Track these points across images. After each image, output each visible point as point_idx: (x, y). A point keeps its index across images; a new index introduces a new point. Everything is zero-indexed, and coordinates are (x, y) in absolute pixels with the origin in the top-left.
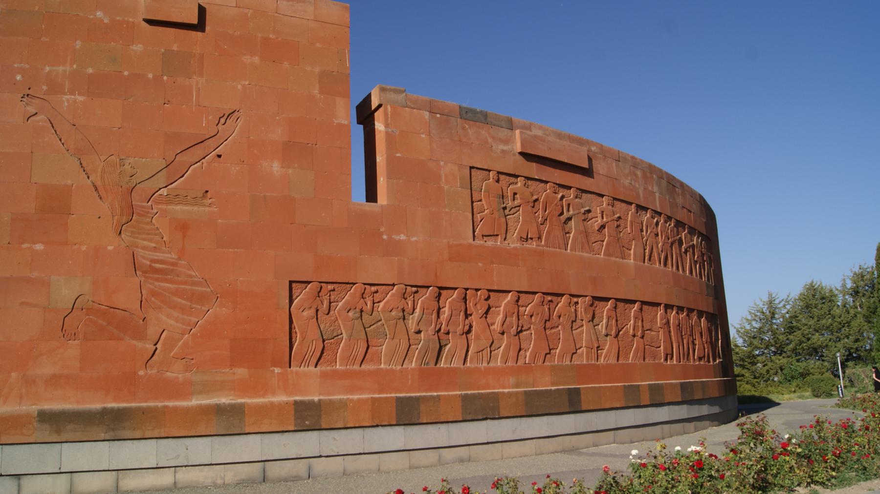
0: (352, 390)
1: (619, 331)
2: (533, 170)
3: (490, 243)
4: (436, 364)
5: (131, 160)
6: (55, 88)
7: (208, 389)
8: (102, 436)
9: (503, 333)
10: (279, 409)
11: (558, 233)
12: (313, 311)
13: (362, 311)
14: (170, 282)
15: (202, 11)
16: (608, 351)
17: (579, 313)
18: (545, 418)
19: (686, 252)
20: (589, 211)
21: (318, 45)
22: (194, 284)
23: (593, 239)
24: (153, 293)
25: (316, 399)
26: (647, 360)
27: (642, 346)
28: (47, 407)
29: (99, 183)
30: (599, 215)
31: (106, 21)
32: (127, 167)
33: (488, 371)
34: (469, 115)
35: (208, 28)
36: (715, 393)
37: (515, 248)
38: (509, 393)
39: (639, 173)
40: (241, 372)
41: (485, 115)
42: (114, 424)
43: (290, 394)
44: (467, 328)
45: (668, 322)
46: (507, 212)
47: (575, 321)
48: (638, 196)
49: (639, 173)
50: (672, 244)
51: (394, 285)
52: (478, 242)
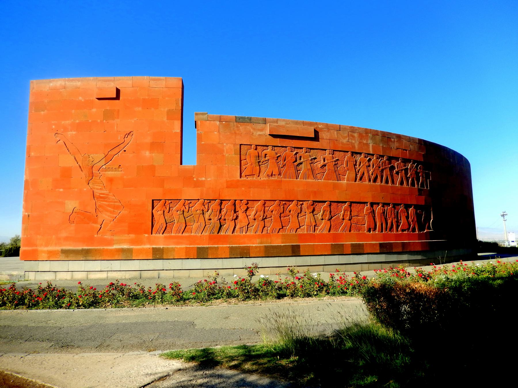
0: (178, 244)
1: (331, 218)
2: (278, 142)
3: (250, 178)
4: (218, 233)
5: (92, 155)
6: (66, 129)
7: (119, 242)
8: (82, 259)
9: (255, 219)
10: (146, 251)
11: (292, 171)
12: (162, 212)
13: (183, 211)
14: (106, 201)
15: (118, 91)
16: (322, 227)
17: (303, 210)
19: (397, 173)
20: (315, 158)
21: (167, 98)
22: (115, 202)
23: (317, 172)
24: (100, 206)
25: (162, 247)
26: (352, 232)
27: (349, 224)
28: (65, 248)
29: (81, 165)
30: (322, 160)
31: (83, 100)
32: (91, 158)
33: (244, 237)
34: (241, 120)
35: (121, 98)
36: (419, 249)
37: (264, 180)
39: (356, 135)
40: (132, 236)
41: (250, 119)
42: (86, 255)
43: (151, 244)
44: (235, 217)
45: (373, 212)
46: (260, 163)
47: (301, 213)
48: (354, 147)
49: (356, 135)
50: (382, 171)
51: (199, 200)
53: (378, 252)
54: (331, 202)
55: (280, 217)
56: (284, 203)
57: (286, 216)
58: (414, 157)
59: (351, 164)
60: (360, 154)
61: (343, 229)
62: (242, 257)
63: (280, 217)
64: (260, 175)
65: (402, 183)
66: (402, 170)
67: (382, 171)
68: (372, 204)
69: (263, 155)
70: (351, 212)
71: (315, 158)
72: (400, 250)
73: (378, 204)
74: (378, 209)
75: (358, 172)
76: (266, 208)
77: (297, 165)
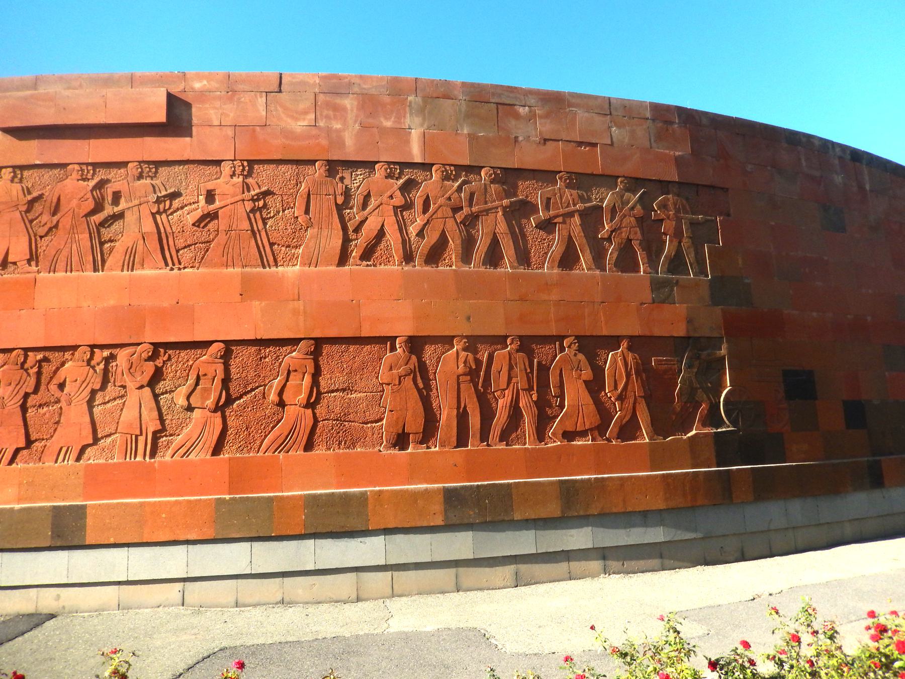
1: (230, 401)
19: (547, 226)
23: (180, 243)
26: (319, 451)
39: (349, 103)
47: (103, 387)
48: (341, 144)
53: (439, 521)
54: (228, 343)
55: (24, 408)
56: (40, 356)
57: (47, 404)
58: (630, 168)
59: (323, 205)
60: (370, 165)
63: (24, 408)
65: (568, 260)
66: (571, 215)
67: (471, 221)
68: (415, 344)
70: (317, 374)
72: (553, 509)
73: (448, 341)
74: (448, 364)
75: (357, 230)
77: (102, 224)
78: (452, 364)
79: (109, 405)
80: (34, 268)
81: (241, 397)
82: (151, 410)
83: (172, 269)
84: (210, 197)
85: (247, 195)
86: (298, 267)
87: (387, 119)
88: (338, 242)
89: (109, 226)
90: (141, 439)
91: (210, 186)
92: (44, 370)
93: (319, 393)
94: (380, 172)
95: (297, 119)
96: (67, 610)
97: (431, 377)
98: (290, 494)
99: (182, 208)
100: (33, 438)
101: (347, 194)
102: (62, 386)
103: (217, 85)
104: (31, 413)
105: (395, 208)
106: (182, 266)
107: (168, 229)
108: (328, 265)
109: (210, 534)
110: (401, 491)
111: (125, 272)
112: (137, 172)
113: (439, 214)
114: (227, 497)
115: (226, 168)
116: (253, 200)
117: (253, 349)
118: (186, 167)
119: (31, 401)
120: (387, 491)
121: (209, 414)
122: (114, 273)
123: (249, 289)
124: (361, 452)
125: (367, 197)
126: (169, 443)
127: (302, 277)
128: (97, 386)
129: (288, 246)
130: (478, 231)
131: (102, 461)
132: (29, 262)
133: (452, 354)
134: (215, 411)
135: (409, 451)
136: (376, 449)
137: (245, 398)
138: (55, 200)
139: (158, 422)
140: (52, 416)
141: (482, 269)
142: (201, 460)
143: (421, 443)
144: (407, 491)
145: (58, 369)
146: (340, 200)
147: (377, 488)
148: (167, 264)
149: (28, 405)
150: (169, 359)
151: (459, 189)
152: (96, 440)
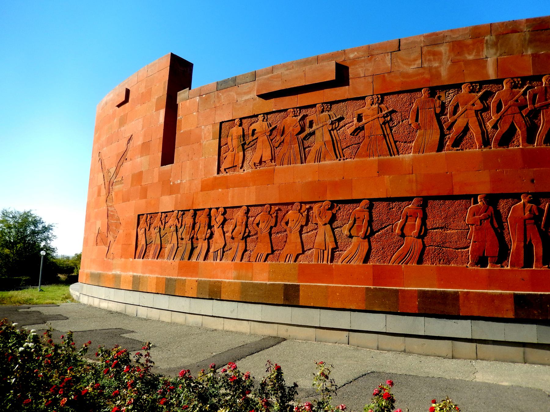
1: (373, 233)
2: (272, 105)
3: (230, 173)
16: (350, 252)
18: (260, 306)
20: (342, 119)
23: (344, 145)
26: (427, 264)
38: (229, 282)
39: (443, 49)
41: (234, 79)
43: (133, 272)
44: (208, 235)
46: (246, 146)
47: (307, 224)
48: (438, 75)
51: (173, 211)
52: (223, 174)
53: (511, 315)
54: (371, 201)
55: (270, 234)
57: (280, 232)
59: (427, 115)
60: (458, 87)
61: (401, 258)
62: (212, 299)
63: (270, 234)
64: (244, 165)
69: (251, 132)
71: (342, 119)
73: (516, 197)
75: (450, 128)
76: (251, 219)
78: (520, 212)
79: (309, 234)
80: (274, 164)
81: (378, 231)
82: (330, 237)
83: (340, 160)
84: (360, 118)
85: (380, 114)
86: (411, 154)
87: (469, 54)
88: (436, 137)
89: (308, 139)
90: (326, 252)
91: (359, 112)
92: (279, 215)
93: (426, 230)
94: (464, 90)
95: (410, 65)
96: (291, 337)
97: (504, 221)
98: (409, 288)
99: (345, 126)
100: (275, 249)
101: (443, 106)
102: (287, 223)
103: (362, 54)
104: (273, 236)
105: (476, 112)
106: (345, 158)
107: (338, 138)
108: (431, 152)
109: (363, 307)
110: (482, 293)
111: (316, 163)
112: (320, 109)
113: (509, 112)
114: (372, 287)
115: (368, 101)
116: (384, 117)
117: (385, 203)
118: (346, 102)
119: (274, 230)
120: (473, 292)
121: (361, 240)
122: (311, 164)
123: (383, 168)
124: (454, 267)
125: (456, 108)
126: (340, 255)
127: (414, 159)
128: (304, 224)
129: (406, 142)
130: (540, 120)
131: (307, 263)
132: (271, 160)
133: (520, 205)
134: (364, 238)
135: (488, 268)
136: (465, 265)
137: (381, 232)
138: (282, 129)
139: (334, 243)
140: (283, 239)
141: (544, 146)
142: (357, 265)
143: (497, 263)
144: (487, 293)
145: (285, 214)
146: (438, 110)
147: (466, 290)
148: (337, 158)
149: (272, 232)
150: (339, 209)
151: (525, 93)
152: (304, 252)
